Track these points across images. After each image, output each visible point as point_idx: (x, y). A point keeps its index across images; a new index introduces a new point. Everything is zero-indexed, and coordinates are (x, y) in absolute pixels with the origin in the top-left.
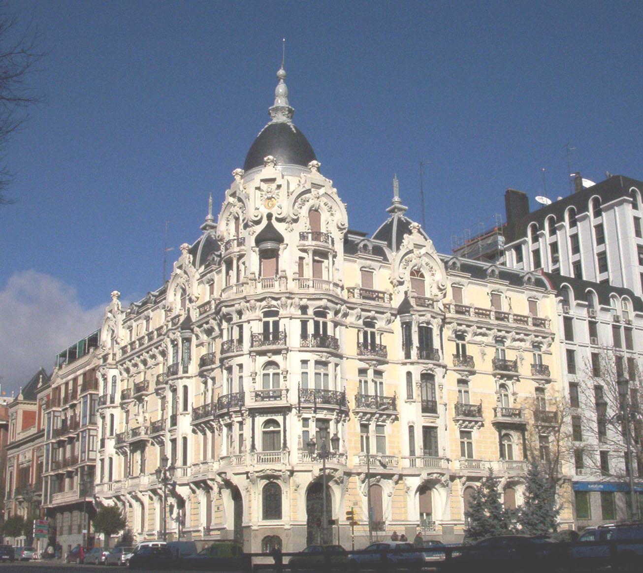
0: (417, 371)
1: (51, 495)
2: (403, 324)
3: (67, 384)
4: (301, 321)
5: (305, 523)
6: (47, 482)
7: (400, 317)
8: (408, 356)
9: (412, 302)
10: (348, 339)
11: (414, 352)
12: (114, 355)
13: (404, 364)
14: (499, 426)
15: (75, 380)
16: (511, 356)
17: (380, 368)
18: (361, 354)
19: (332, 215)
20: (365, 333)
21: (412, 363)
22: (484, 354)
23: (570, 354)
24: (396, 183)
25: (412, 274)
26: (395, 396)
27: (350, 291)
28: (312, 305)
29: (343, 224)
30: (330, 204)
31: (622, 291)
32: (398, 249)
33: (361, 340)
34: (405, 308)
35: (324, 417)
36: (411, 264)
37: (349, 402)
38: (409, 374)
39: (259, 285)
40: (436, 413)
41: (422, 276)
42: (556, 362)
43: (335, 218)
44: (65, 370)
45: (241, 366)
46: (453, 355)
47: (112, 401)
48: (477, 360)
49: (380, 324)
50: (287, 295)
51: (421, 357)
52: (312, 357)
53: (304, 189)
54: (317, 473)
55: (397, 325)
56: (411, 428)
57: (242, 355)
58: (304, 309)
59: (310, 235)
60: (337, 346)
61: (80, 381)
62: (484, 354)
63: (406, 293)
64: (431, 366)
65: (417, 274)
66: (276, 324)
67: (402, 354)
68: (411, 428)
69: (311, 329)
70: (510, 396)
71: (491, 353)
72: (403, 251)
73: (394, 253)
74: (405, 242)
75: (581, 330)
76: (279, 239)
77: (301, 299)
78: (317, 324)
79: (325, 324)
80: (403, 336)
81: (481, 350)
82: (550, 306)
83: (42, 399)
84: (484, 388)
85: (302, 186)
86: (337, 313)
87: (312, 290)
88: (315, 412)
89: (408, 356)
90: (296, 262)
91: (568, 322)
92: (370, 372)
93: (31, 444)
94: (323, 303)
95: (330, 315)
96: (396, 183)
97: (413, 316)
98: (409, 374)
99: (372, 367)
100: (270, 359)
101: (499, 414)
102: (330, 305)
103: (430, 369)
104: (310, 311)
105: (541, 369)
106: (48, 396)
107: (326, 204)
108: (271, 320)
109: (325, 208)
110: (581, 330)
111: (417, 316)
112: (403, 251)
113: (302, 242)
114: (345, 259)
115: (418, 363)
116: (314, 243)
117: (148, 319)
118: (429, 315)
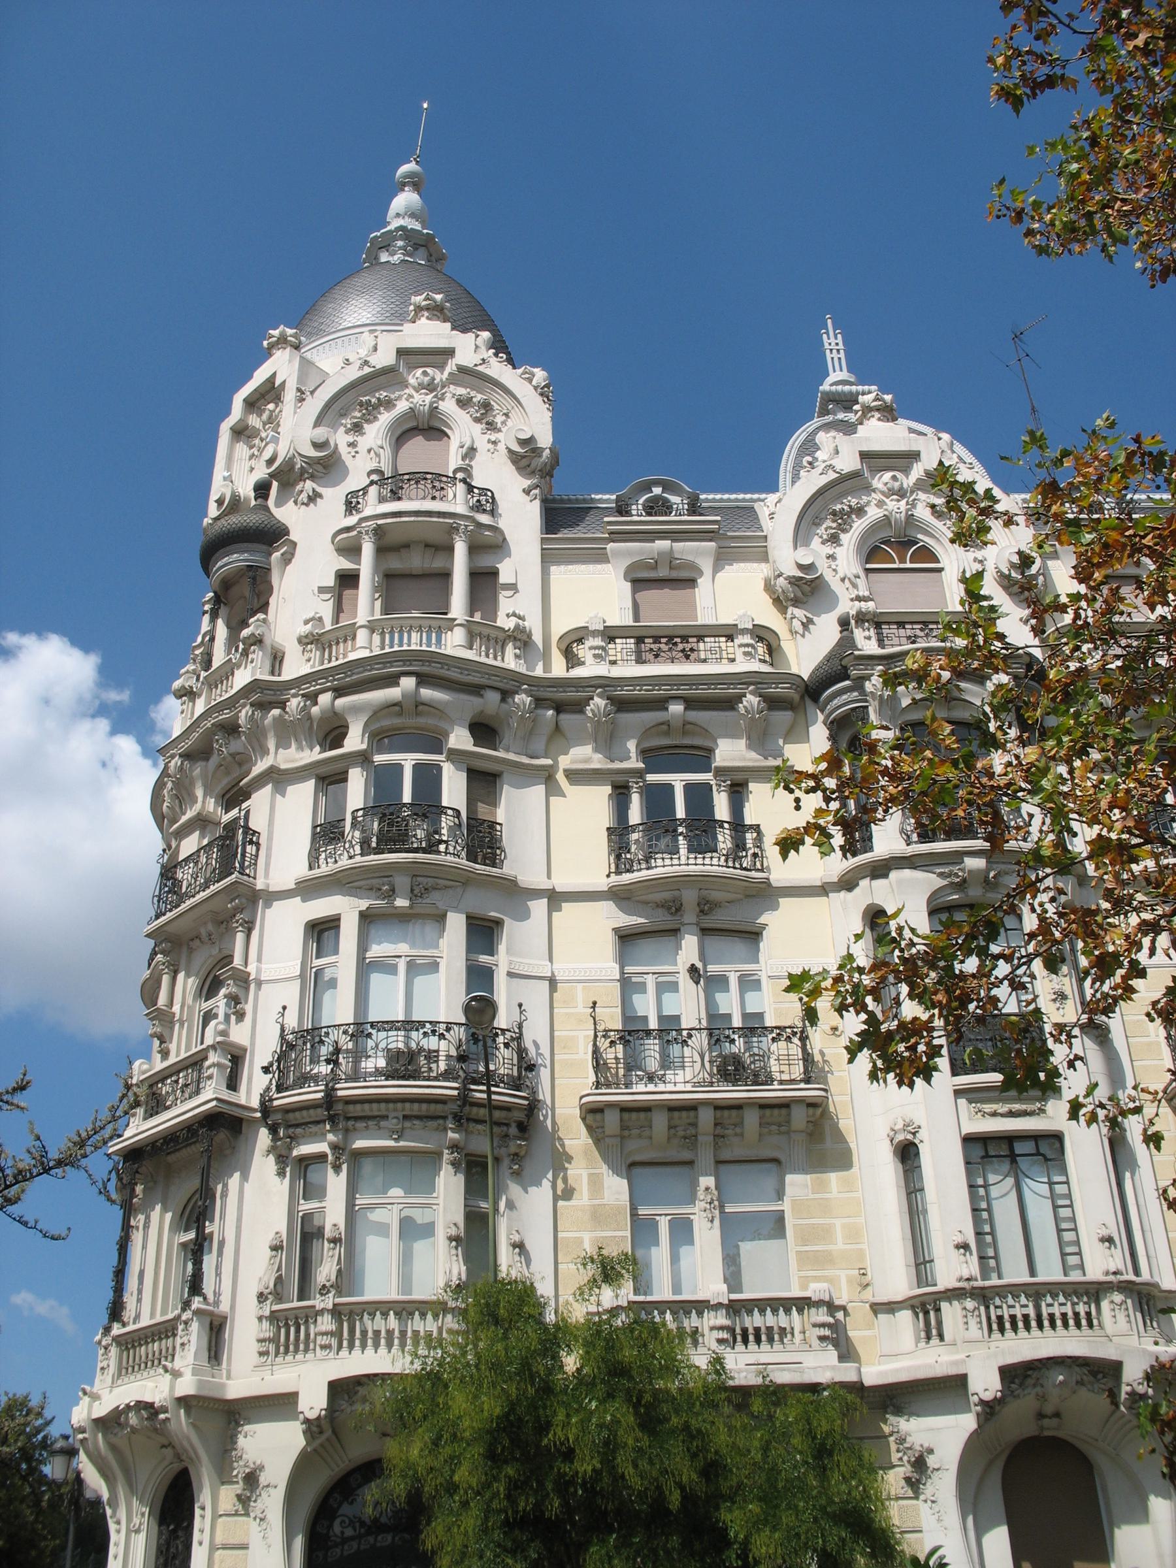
21: (880, 870)
24: (833, 343)
28: (356, 709)
30: (478, 397)
33: (635, 815)
36: (859, 526)
41: (927, 554)
43: (498, 434)
52: (346, 908)
53: (367, 370)
54: (314, 1402)
56: (907, 1153)
68: (907, 1153)
72: (811, 482)
77: (313, 698)
90: (322, 590)
96: (833, 343)
104: (355, 741)
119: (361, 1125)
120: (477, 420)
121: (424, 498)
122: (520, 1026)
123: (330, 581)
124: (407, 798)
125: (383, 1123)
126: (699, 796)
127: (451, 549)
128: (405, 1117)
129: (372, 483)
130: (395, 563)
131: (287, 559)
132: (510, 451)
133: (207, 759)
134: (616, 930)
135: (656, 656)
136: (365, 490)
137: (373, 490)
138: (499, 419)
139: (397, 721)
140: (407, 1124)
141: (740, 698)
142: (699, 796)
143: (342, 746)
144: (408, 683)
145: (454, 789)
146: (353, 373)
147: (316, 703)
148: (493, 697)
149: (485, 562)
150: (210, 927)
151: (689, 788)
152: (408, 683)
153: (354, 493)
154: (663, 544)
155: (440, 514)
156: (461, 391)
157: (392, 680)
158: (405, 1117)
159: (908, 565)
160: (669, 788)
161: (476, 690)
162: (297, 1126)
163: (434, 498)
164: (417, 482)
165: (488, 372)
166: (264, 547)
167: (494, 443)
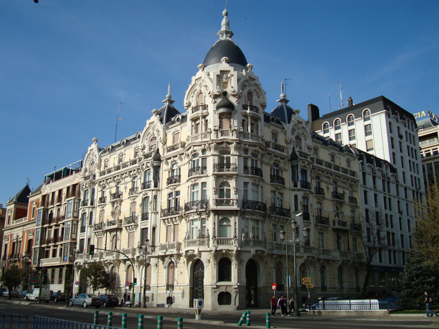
0: (300, 195)
1: (39, 259)
2: (292, 167)
3: (53, 193)
5: (245, 284)
6: (35, 252)
8: (295, 185)
9: (298, 154)
10: (267, 172)
11: (299, 184)
12: (94, 176)
13: (293, 190)
14: (336, 230)
15: (60, 191)
16: (340, 191)
17: (281, 191)
18: (272, 181)
19: (258, 97)
21: (298, 190)
22: (328, 188)
23: (365, 192)
25: (296, 138)
26: (290, 209)
27: (267, 144)
31: (385, 162)
32: (289, 122)
34: (294, 157)
38: (296, 197)
39: (219, 134)
40: (309, 220)
41: (300, 140)
42: (359, 196)
44: (52, 184)
45: (204, 184)
47: (92, 203)
48: (325, 191)
49: (281, 165)
50: (237, 141)
51: (302, 186)
57: (207, 176)
58: (246, 151)
60: (262, 176)
61: (65, 191)
62: (328, 188)
63: (293, 149)
64: (308, 192)
65: (298, 138)
66: (228, 159)
67: (292, 184)
69: (249, 164)
70: (339, 213)
71: (332, 188)
73: (288, 125)
74: (293, 119)
75: (369, 179)
77: (245, 145)
78: (252, 160)
79: (256, 161)
81: (327, 186)
82: (356, 166)
83: (32, 202)
84: (328, 208)
86: (262, 155)
87: (250, 140)
88: (252, 214)
89: (295, 185)
91: (364, 174)
93: (22, 228)
94: (257, 148)
95: (260, 157)
97: (299, 162)
98: (296, 197)
101: (336, 224)
102: (260, 150)
103: (308, 195)
104: (249, 154)
105: (353, 200)
106: (38, 199)
107: (255, 90)
108: (225, 156)
109: (255, 92)
110: (369, 179)
111: (301, 162)
112: (292, 124)
113: (244, 111)
115: (301, 190)
116: (252, 112)
117: (121, 155)
118: (306, 163)
144: (258, 148)
152: (258, 148)
154: (276, 128)
156: (255, 88)
157: (256, 146)
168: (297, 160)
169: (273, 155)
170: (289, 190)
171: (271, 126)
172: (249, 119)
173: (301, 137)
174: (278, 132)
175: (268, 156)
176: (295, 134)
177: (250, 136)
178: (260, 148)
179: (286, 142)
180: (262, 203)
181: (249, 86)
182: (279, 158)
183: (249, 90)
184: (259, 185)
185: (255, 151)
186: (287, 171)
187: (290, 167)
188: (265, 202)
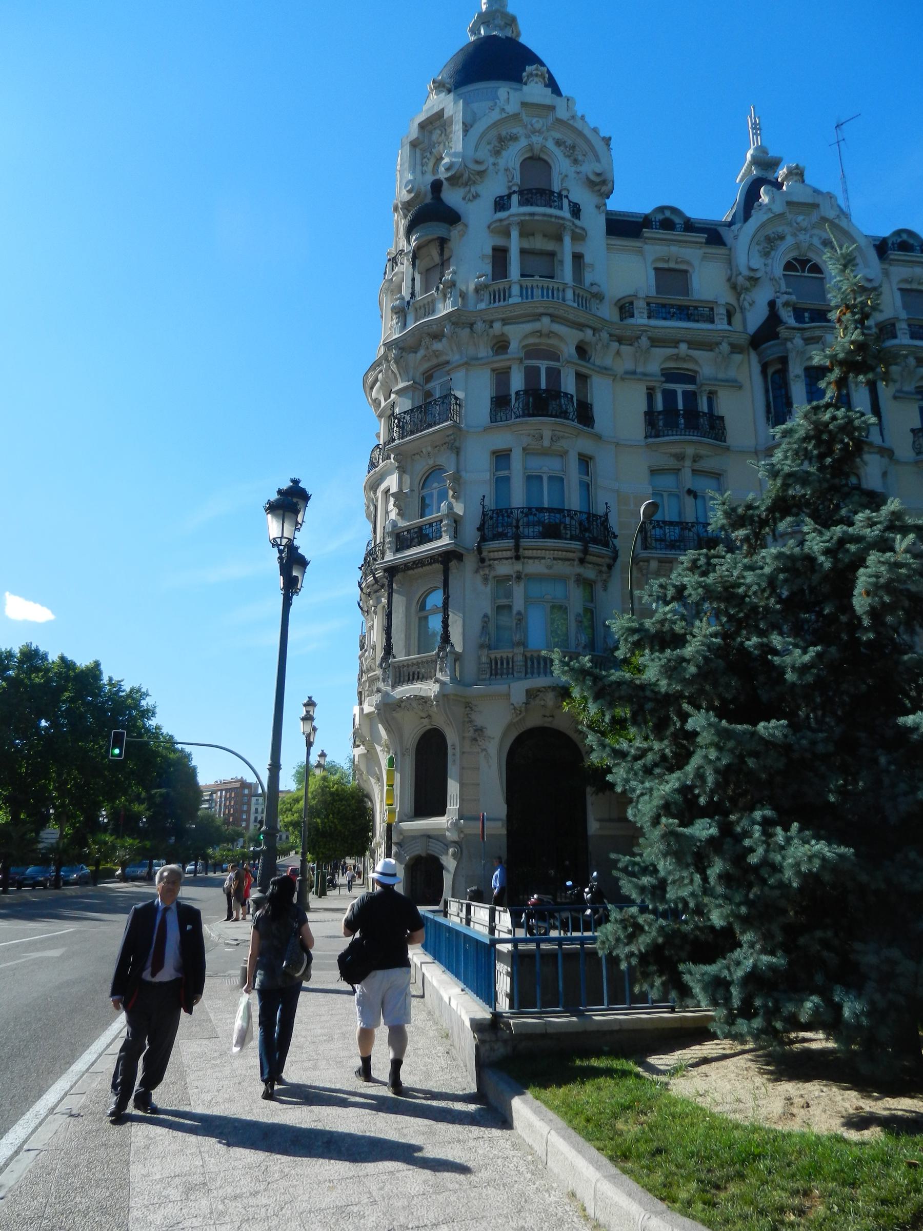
4: (493, 370)
7: (759, 355)
19: (576, 161)
20: (670, 396)
27: (625, 308)
29: (598, 171)
33: (659, 406)
35: (546, 571)
36: (783, 247)
37: (615, 537)
46: (913, 430)
53: (504, 115)
55: (748, 371)
59: (515, 198)
63: (772, 304)
76: (452, 218)
79: (554, 375)
80: (767, 391)
85: (497, 110)
92: (687, 473)
99: (688, 463)
100: (431, 462)
114: (609, 248)
119: (531, 561)
120: (569, 157)
121: (545, 206)
122: (607, 515)
123: (489, 252)
124: (543, 386)
125: (543, 561)
126: (691, 397)
127: (559, 239)
128: (554, 559)
129: (514, 192)
130: (526, 245)
131: (463, 234)
132: (588, 178)
133: (416, 352)
134: (649, 467)
135: (673, 316)
136: (509, 196)
137: (515, 198)
138: (580, 158)
139: (537, 341)
140: (555, 562)
141: (718, 344)
142: (691, 397)
143: (507, 353)
144: (546, 320)
145: (569, 385)
146: (495, 116)
147: (491, 327)
148: (589, 332)
149: (579, 249)
150: (429, 449)
151: (685, 393)
152: (546, 320)
153: (501, 197)
155: (556, 217)
156: (558, 135)
158: (554, 559)
159: (806, 274)
160: (674, 392)
161: (580, 326)
162: (495, 560)
163: (551, 207)
164: (541, 196)
165: (576, 125)
166: (446, 226)
167: (578, 173)
168: (776, 336)
169: (644, 341)
170: (756, 453)
171: (646, 247)
172: (515, 234)
173: (815, 259)
174: (688, 263)
175: (624, 348)
176: (783, 253)
177: (515, 290)
178: (554, 318)
179: (734, 287)
180: (591, 517)
181: (528, 137)
182: (683, 347)
183: (531, 147)
184: (566, 452)
185: (539, 333)
186: (740, 387)
187: (756, 368)
188: (601, 511)
